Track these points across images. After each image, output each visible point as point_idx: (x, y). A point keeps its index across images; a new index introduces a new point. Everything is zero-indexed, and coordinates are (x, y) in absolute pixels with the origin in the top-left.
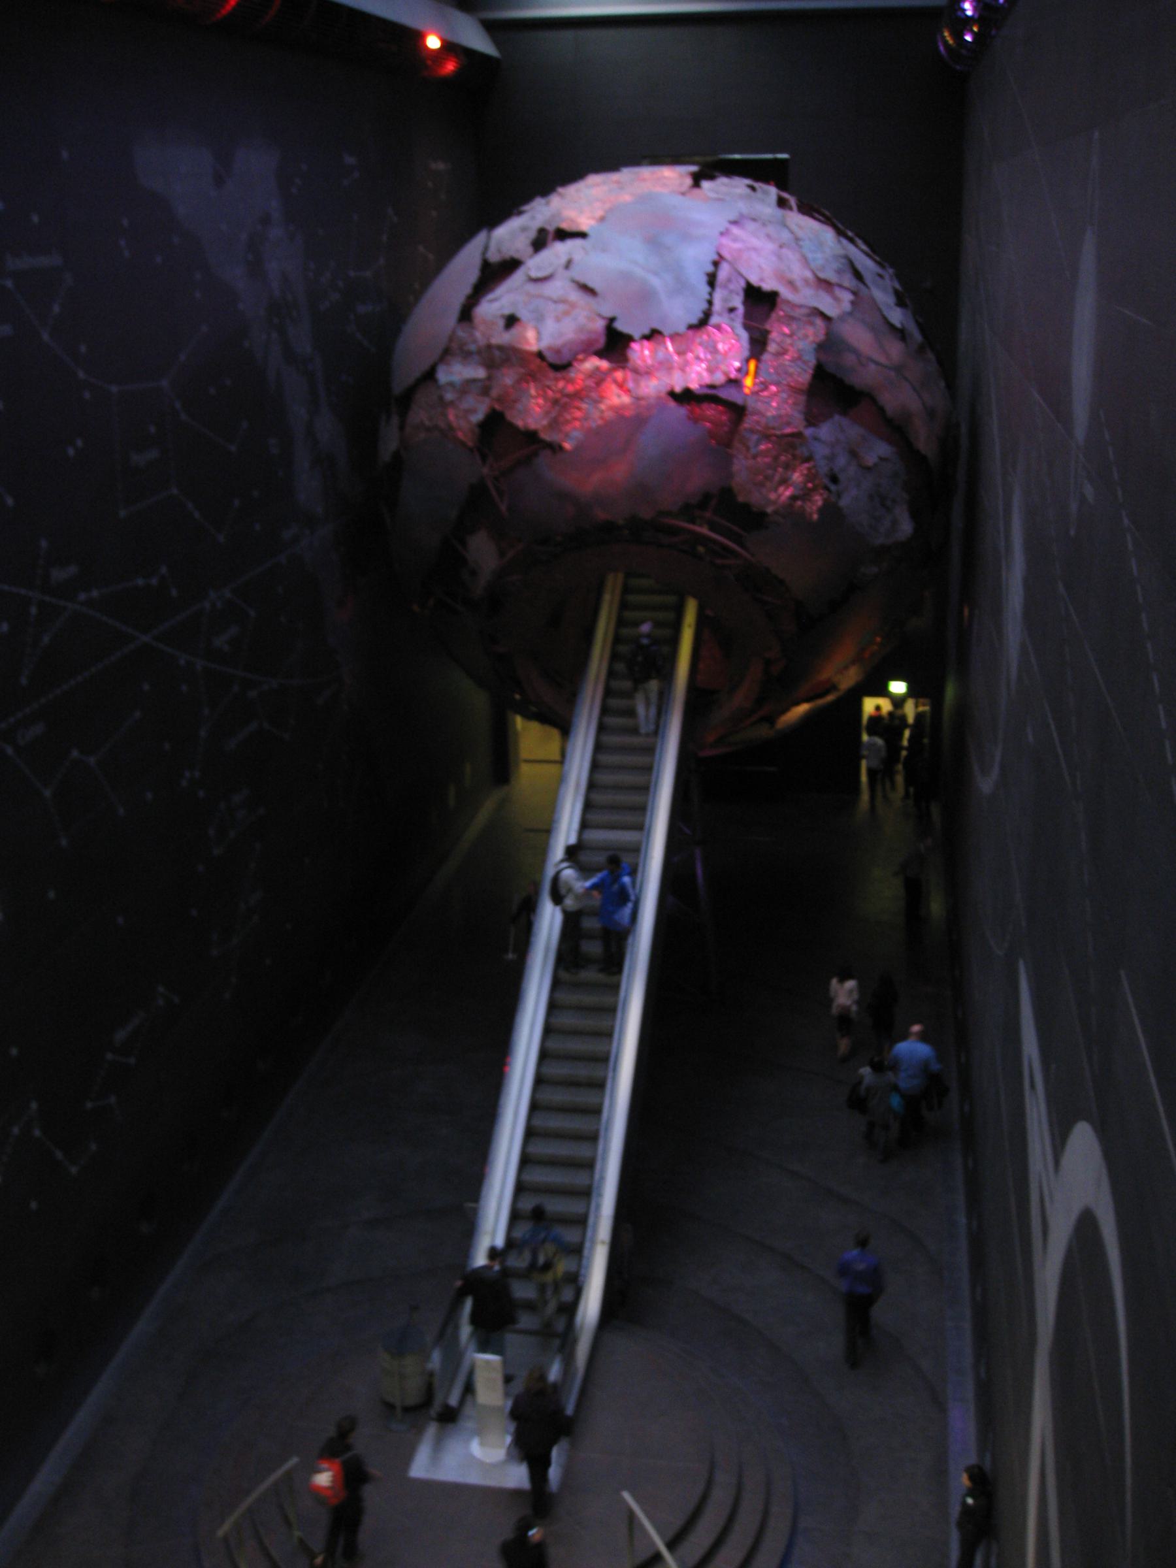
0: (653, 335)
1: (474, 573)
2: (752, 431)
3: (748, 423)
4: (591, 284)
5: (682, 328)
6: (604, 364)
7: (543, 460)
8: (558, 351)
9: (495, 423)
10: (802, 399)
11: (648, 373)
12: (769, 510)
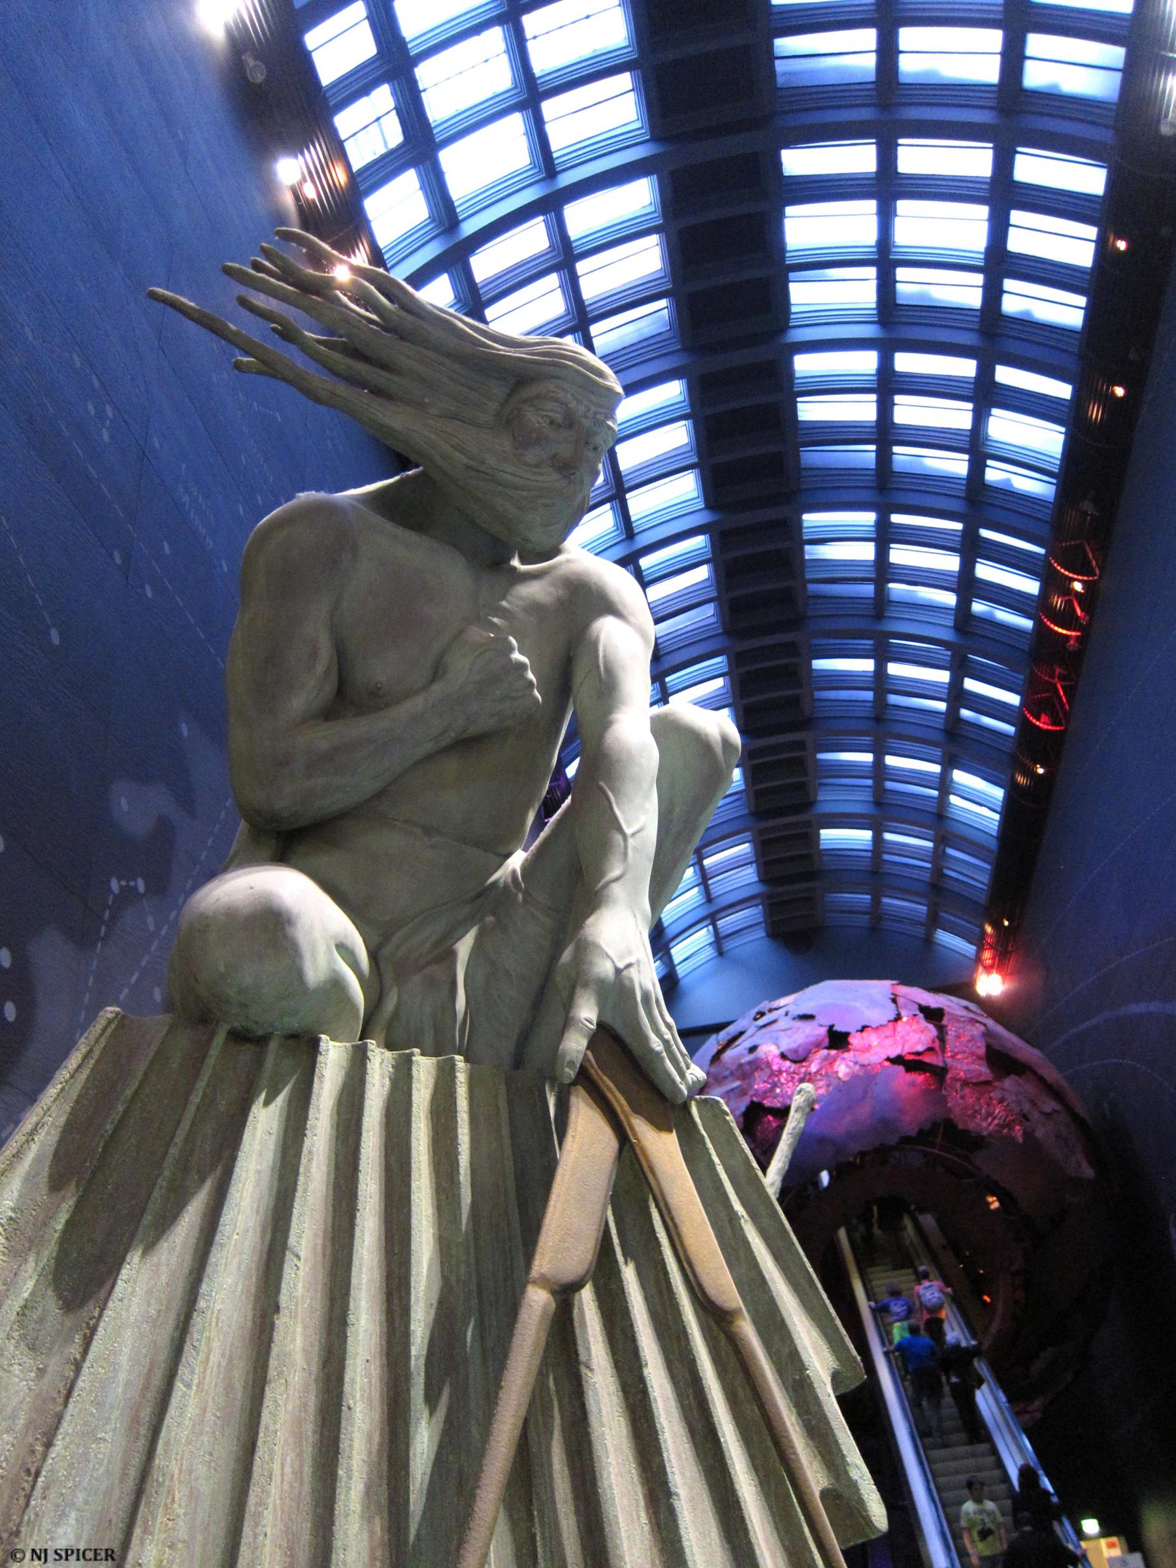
0: (864, 1028)
4: (809, 1012)
6: (833, 1052)
8: (796, 1051)
10: (985, 1062)
11: (868, 1048)
12: (985, 1133)
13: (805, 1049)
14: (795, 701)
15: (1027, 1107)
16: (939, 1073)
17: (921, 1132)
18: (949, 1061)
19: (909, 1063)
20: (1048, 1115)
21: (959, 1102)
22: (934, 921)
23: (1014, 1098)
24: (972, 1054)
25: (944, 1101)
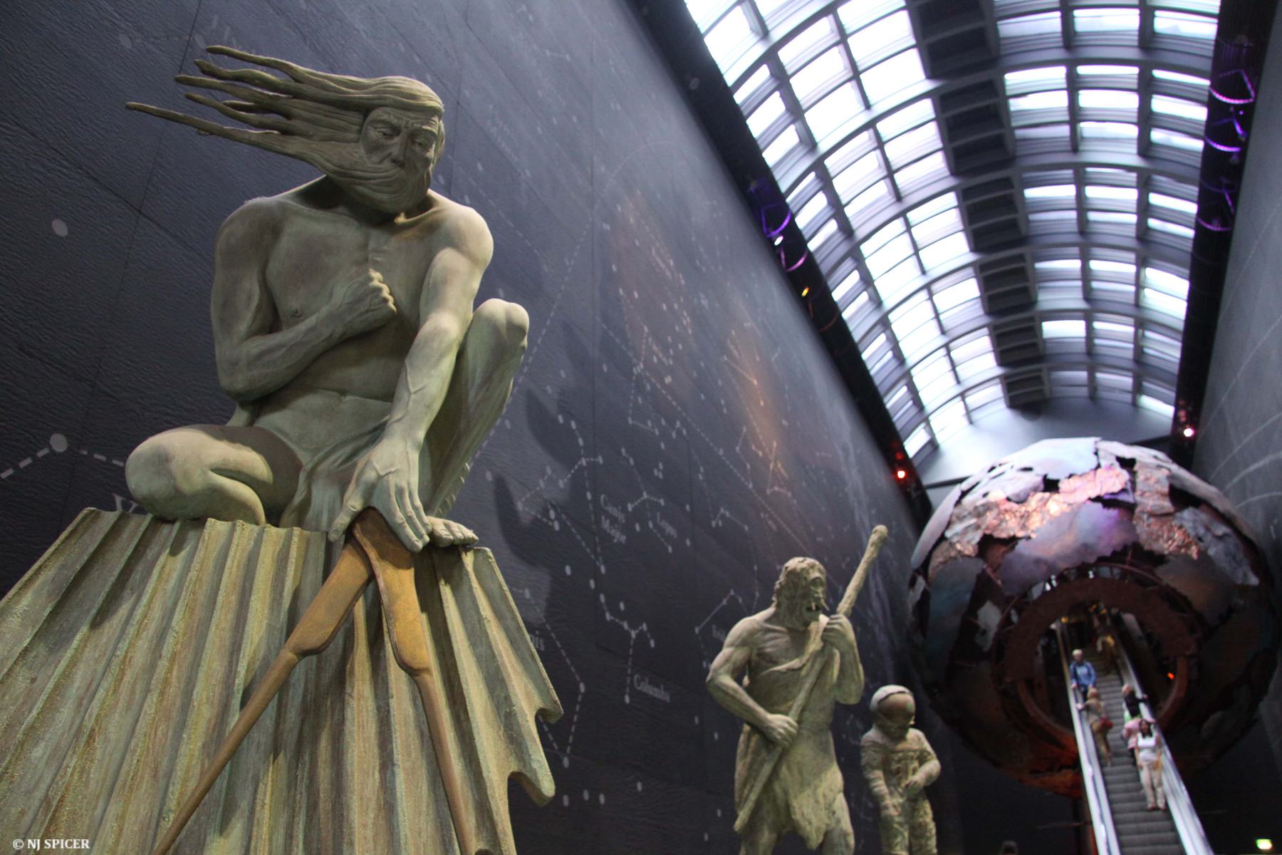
1: (984, 632)
2: (1143, 512)
3: (1138, 510)
6: (1047, 494)
7: (1021, 546)
8: (1018, 495)
9: (987, 542)
10: (1167, 498)
11: (1073, 491)
12: (1166, 552)
14: (1013, 225)
15: (1201, 531)
16: (1129, 508)
17: (1114, 553)
18: (1138, 499)
19: (1107, 502)
20: (1220, 538)
21: (1144, 528)
22: (1138, 389)
24: (1158, 492)
25: (1133, 528)
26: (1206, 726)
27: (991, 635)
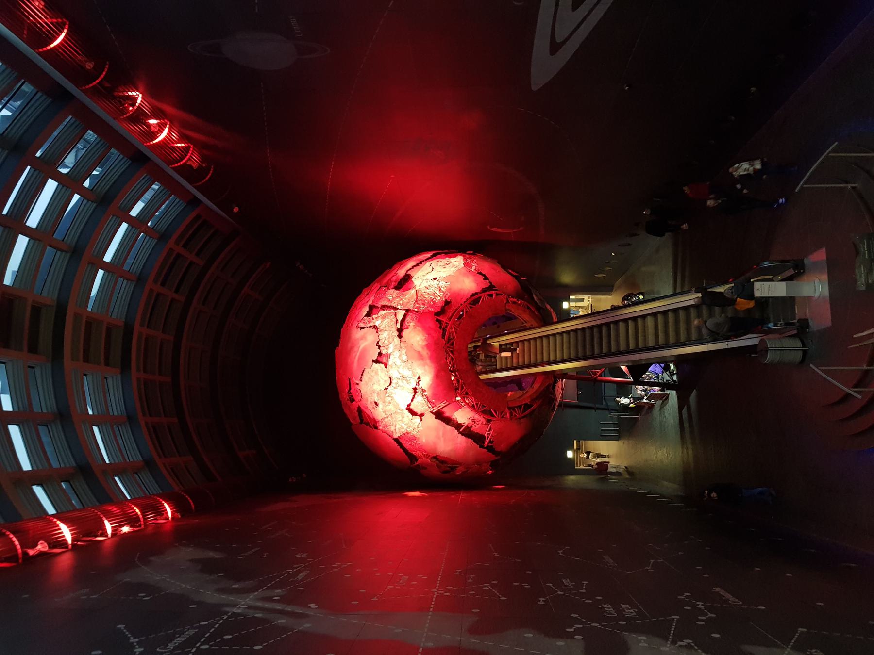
5: (377, 334)
13: (385, 377)
17: (440, 327)
23: (425, 281)
26: (540, 305)
27: (477, 417)
